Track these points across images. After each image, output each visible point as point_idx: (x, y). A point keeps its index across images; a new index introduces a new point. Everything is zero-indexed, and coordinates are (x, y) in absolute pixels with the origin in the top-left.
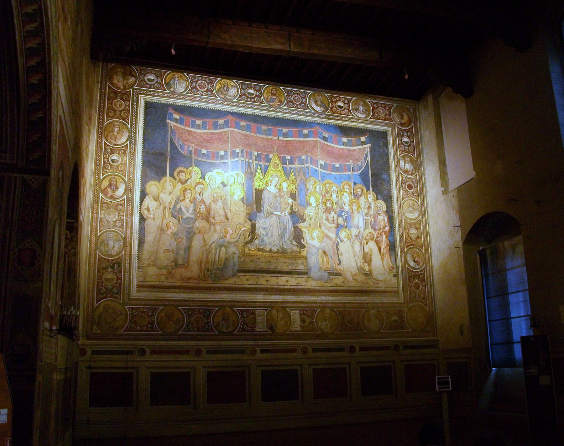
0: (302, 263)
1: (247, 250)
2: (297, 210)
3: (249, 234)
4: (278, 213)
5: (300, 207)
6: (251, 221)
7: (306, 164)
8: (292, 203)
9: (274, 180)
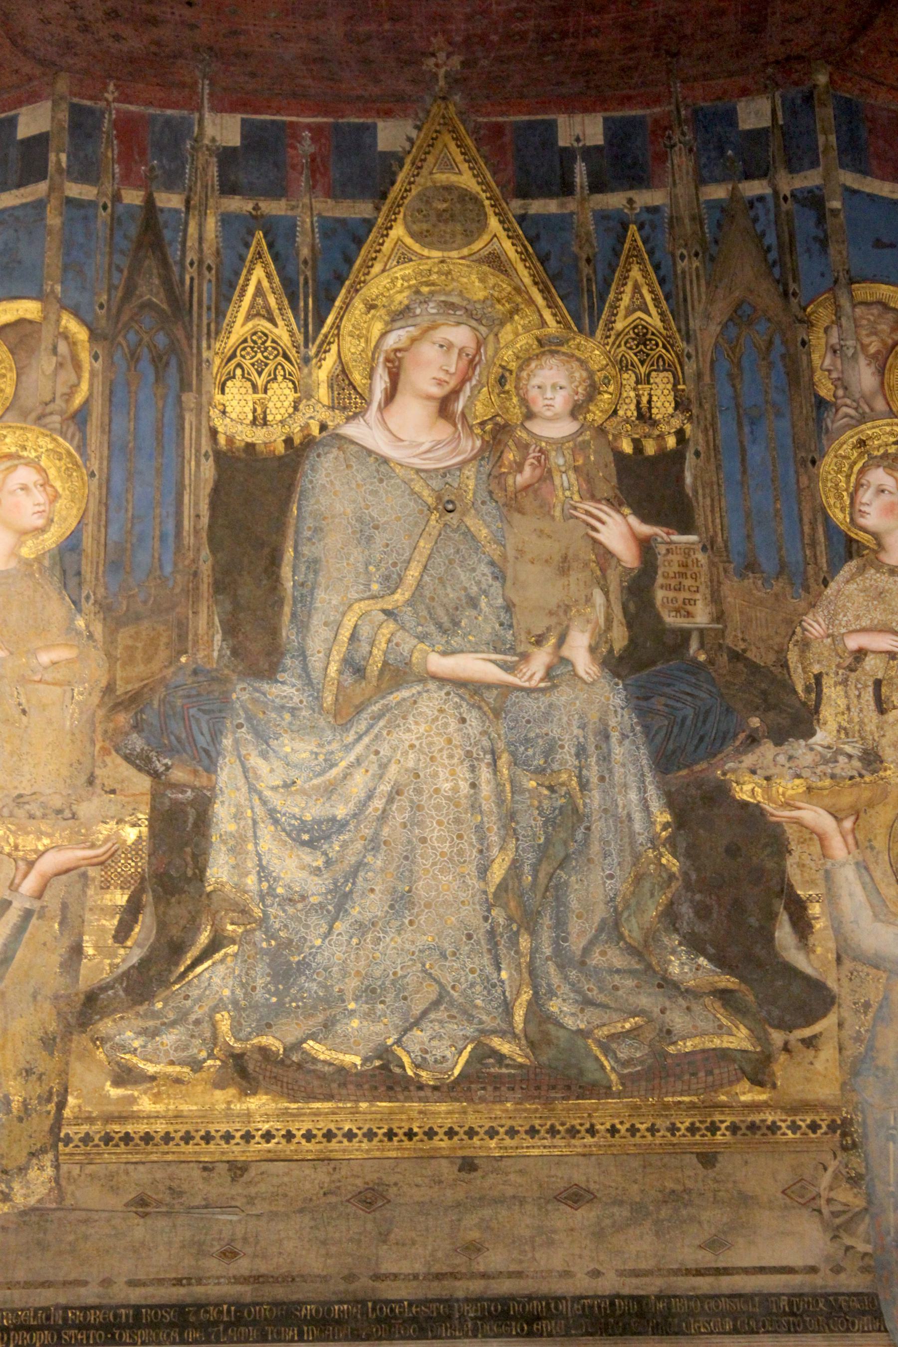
0: (800, 1196)
1: (92, 1089)
2: (702, 616)
3: (133, 909)
4: (477, 666)
5: (732, 589)
6: (155, 775)
7: (792, 168)
8: (645, 546)
9: (429, 351)
